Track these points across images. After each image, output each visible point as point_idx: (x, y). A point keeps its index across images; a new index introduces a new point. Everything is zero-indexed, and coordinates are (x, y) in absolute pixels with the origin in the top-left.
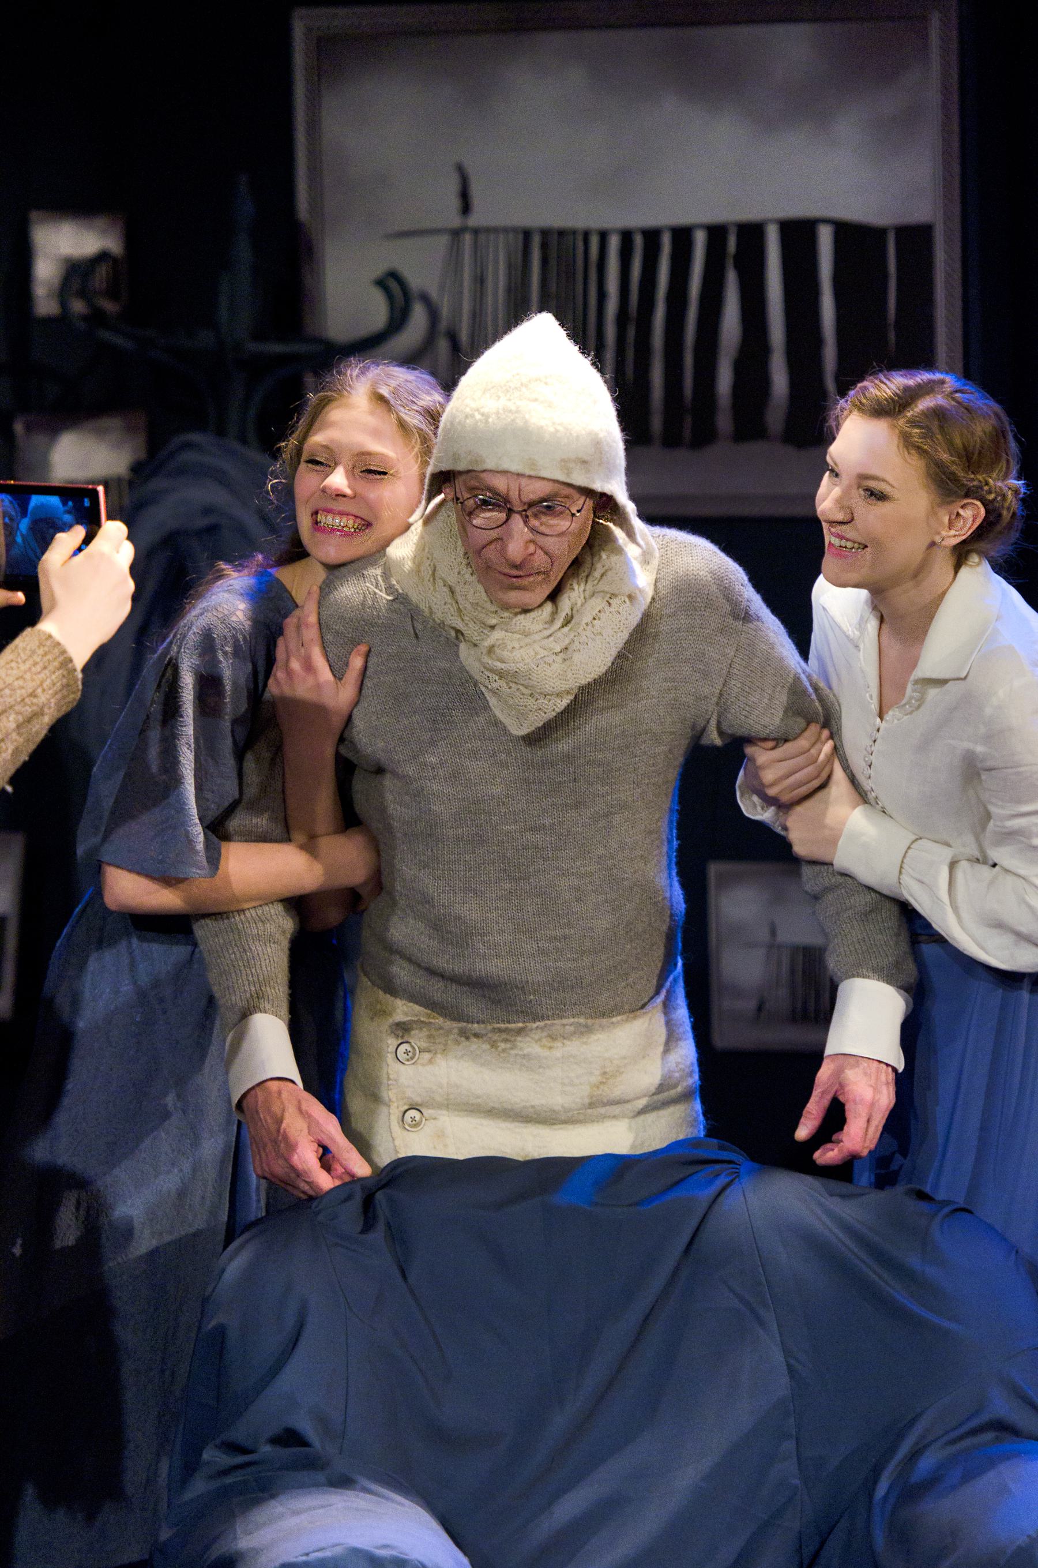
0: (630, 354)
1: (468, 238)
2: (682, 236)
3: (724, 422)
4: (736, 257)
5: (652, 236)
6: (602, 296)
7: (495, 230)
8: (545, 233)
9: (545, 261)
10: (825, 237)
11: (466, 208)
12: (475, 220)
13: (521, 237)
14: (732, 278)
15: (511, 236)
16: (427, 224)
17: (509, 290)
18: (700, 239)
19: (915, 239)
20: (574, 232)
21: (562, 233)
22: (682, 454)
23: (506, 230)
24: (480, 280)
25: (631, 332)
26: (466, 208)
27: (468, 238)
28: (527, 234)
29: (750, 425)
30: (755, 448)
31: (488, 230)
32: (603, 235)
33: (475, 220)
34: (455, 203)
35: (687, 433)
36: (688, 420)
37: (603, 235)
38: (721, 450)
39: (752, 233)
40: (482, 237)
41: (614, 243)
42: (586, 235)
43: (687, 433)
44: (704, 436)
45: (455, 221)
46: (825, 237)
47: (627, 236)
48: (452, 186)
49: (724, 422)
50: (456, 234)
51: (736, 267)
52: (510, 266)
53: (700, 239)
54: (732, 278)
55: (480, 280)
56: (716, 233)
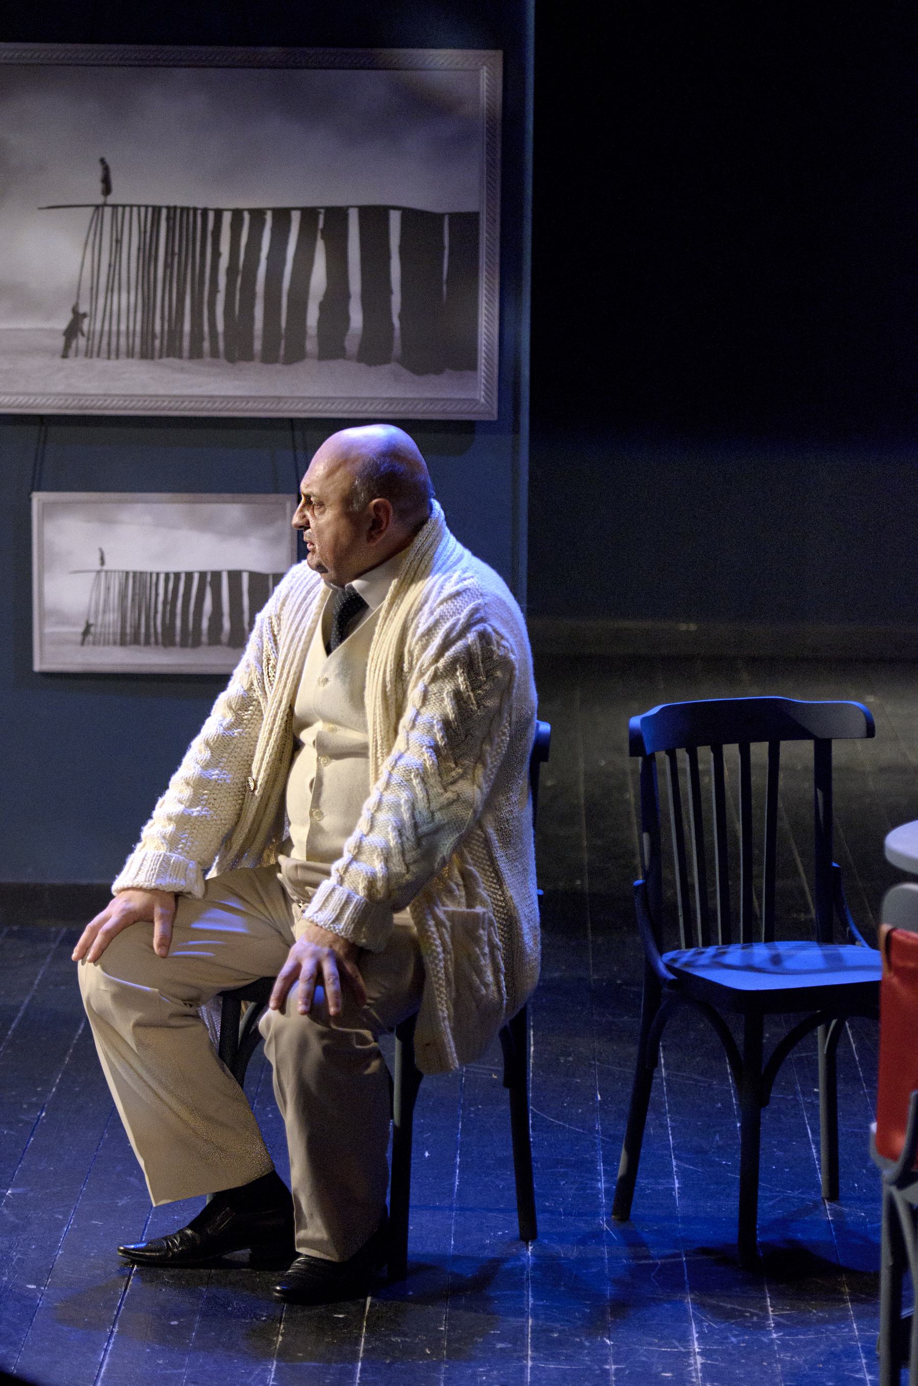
1: (108, 211)
7: (131, 206)
10: (395, 219)
11: (107, 190)
12: (111, 200)
13: (150, 210)
15: (143, 210)
19: (465, 223)
20: (195, 209)
22: (278, 366)
23: (139, 206)
24: (119, 242)
26: (107, 190)
27: (108, 211)
28: (157, 210)
29: (332, 347)
30: (337, 365)
31: (124, 206)
32: (219, 213)
33: (111, 200)
34: (99, 186)
35: (282, 352)
38: (310, 364)
42: (205, 212)
43: (282, 352)
45: (100, 200)
46: (395, 219)
48: (98, 173)
52: (142, 233)
54: (320, 246)
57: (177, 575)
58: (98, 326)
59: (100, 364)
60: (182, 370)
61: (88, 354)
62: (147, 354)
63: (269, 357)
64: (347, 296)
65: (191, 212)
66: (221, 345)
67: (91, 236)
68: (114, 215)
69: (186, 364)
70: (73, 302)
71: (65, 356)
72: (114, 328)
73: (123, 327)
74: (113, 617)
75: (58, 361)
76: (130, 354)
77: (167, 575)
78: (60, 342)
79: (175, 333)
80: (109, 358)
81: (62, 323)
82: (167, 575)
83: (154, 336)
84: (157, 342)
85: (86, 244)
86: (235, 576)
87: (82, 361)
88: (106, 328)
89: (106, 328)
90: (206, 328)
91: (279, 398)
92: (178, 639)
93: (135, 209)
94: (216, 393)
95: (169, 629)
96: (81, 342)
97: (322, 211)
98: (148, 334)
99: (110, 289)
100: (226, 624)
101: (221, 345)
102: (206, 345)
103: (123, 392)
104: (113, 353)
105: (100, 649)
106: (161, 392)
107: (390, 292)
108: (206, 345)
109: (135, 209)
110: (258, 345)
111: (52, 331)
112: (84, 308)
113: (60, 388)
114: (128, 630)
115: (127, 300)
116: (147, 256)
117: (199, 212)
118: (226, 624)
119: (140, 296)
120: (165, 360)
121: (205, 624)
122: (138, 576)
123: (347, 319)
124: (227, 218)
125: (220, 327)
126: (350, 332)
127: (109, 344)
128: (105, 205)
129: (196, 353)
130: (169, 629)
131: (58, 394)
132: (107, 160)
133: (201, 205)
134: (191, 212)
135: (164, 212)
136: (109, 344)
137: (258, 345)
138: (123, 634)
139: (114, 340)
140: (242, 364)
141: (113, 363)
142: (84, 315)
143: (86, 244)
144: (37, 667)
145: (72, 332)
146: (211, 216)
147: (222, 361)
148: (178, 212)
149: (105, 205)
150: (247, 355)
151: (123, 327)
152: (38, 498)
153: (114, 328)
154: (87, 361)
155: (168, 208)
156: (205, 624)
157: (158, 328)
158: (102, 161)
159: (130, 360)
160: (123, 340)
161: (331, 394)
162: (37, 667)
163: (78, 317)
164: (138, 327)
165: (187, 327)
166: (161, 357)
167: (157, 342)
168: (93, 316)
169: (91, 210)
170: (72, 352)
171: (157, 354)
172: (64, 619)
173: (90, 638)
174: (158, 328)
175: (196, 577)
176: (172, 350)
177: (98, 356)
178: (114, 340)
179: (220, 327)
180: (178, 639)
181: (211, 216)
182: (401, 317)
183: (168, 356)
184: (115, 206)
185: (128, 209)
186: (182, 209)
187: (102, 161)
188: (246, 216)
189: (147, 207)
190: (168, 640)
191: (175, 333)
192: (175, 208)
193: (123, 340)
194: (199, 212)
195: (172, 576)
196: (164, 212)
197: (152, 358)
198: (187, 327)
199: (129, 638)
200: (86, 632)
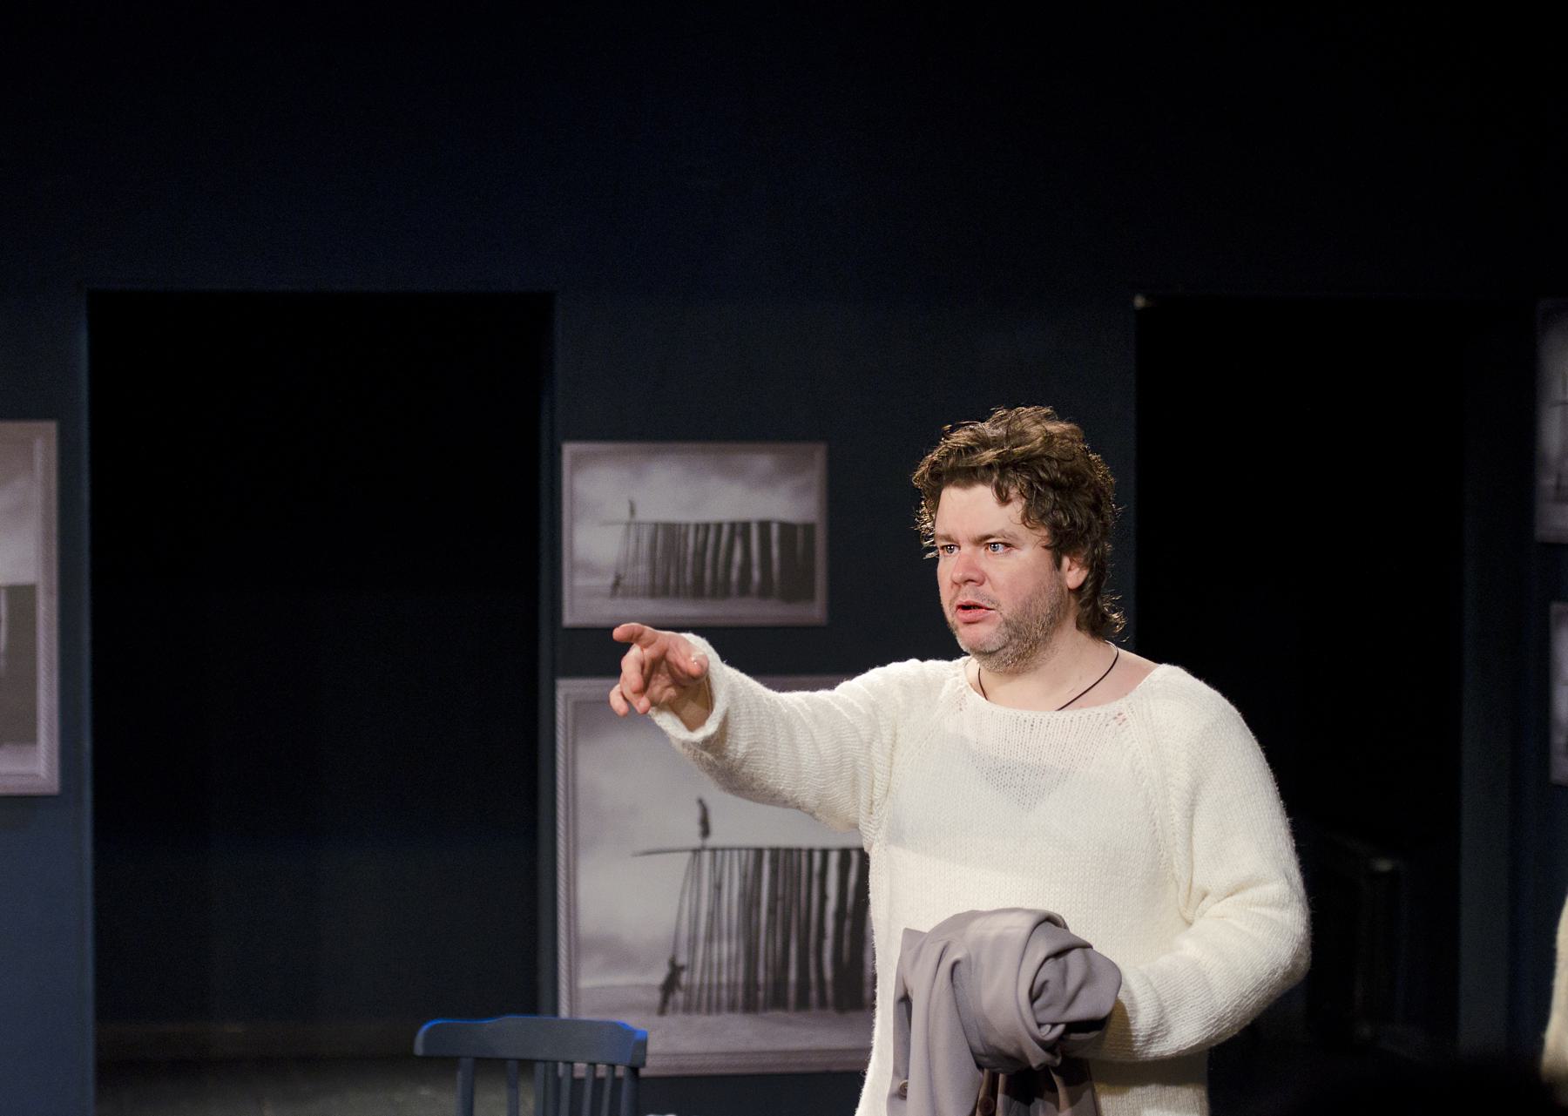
0: (846, 943)
1: (707, 855)
7: (731, 849)
8: (775, 851)
11: (706, 831)
13: (752, 854)
16: (677, 844)
17: (743, 895)
20: (800, 850)
21: (789, 851)
23: (740, 849)
24: (718, 887)
25: (848, 925)
26: (706, 831)
27: (707, 855)
28: (759, 852)
31: (723, 849)
32: (825, 853)
34: (696, 828)
37: (825, 853)
40: (719, 853)
41: (834, 858)
42: (810, 852)
45: (697, 842)
48: (696, 813)
50: (696, 852)
52: (744, 877)
55: (718, 887)
59: (700, 1020)
60: (789, 1023)
61: (687, 1009)
66: (830, 993)
68: (714, 859)
70: (668, 955)
71: (662, 1011)
72: (715, 980)
73: (724, 979)
76: (732, 1007)
78: (657, 997)
79: (779, 985)
80: (709, 1011)
81: (659, 976)
83: (757, 987)
87: (680, 1016)
96: (679, 996)
98: (751, 985)
99: (709, 939)
101: (830, 993)
102: (814, 994)
104: (714, 1007)
108: (814, 994)
111: (648, 987)
112: (682, 960)
120: (770, 1014)
129: (803, 1003)
135: (767, 855)
136: (709, 998)
140: (852, 1015)
141: (712, 1020)
142: (682, 968)
145: (670, 985)
146: (817, 857)
147: (831, 1011)
158: (701, 802)
159: (731, 1016)
160: (724, 994)
163: (675, 970)
164: (741, 979)
165: (793, 975)
166: (765, 1009)
167: (761, 994)
168: (690, 967)
169: (688, 855)
170: (670, 1007)
171: (761, 1004)
176: (778, 1000)
181: (817, 857)
184: (714, 850)
187: (701, 802)
189: (747, 849)
191: (779, 985)
196: (767, 855)
198: (793, 975)
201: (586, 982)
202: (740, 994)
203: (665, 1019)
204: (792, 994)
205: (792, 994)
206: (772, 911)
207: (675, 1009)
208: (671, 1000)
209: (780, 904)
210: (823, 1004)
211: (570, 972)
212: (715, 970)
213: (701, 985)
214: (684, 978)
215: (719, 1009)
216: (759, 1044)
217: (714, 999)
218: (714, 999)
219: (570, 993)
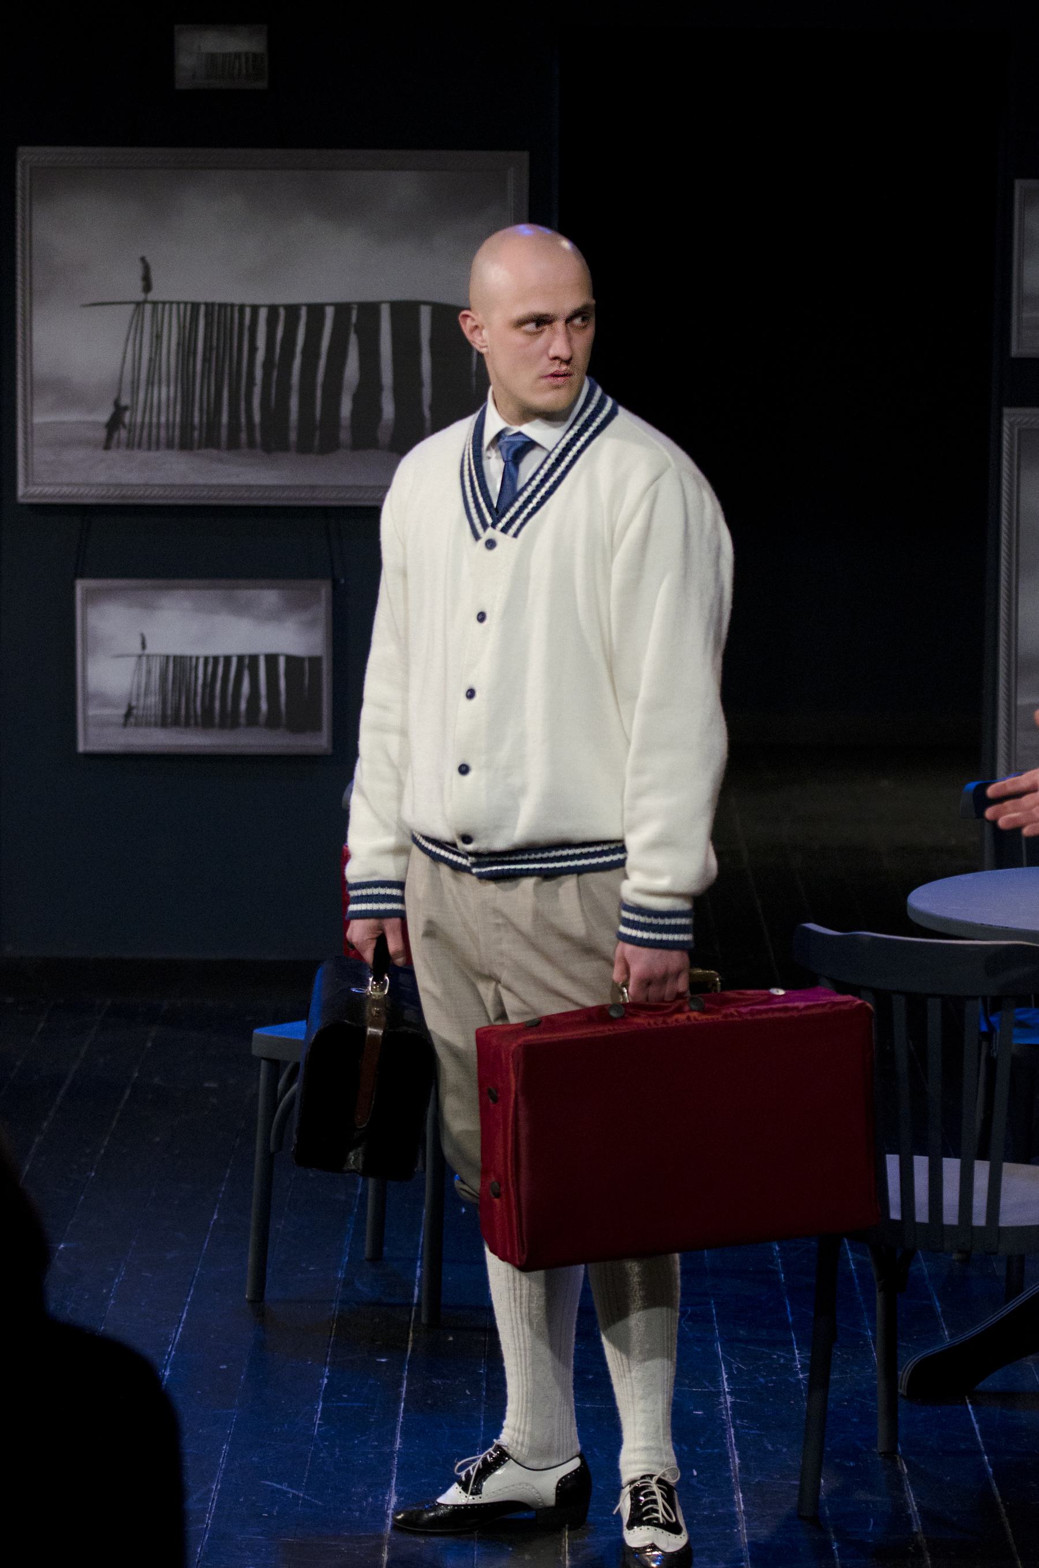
1: (148, 308)
2: (316, 311)
3: (345, 436)
4: (355, 326)
5: (292, 310)
6: (253, 349)
7: (171, 303)
9: (208, 325)
10: (425, 313)
11: (147, 287)
12: (152, 296)
13: (189, 307)
14: (353, 339)
15: (182, 306)
18: (330, 312)
20: (232, 306)
21: (222, 306)
23: (178, 303)
24: (159, 337)
26: (147, 287)
27: (148, 308)
28: (195, 306)
31: (164, 303)
32: (255, 309)
33: (152, 296)
34: (140, 284)
35: (316, 442)
36: (318, 433)
37: (255, 309)
39: (370, 310)
40: (160, 306)
41: (263, 313)
42: (242, 307)
43: (316, 442)
44: (329, 445)
45: (140, 297)
46: (425, 313)
47: (273, 310)
48: (138, 271)
49: (345, 436)
50: (138, 304)
51: (356, 332)
52: (181, 328)
53: (330, 312)
54: (353, 339)
56: (342, 309)
57: (216, 659)
58: (139, 419)
59: (141, 455)
60: (220, 460)
61: (130, 445)
62: (186, 445)
63: (304, 448)
64: (379, 388)
65: (229, 309)
67: (132, 332)
69: (224, 455)
70: (115, 396)
71: (107, 447)
72: (154, 420)
73: (163, 419)
74: (153, 700)
75: (101, 453)
76: (170, 445)
77: (206, 659)
78: (102, 434)
79: (212, 424)
80: (149, 449)
81: (104, 416)
82: (206, 659)
83: (193, 428)
84: (196, 434)
85: (127, 340)
86: (272, 659)
88: (147, 419)
89: (147, 419)
90: (243, 420)
91: (313, 487)
92: (217, 720)
93: (174, 306)
94: (253, 482)
95: (208, 710)
96: (123, 434)
97: (355, 306)
98: (187, 425)
99: (150, 383)
100: (264, 706)
102: (243, 436)
103: (164, 482)
104: (154, 444)
105: (142, 731)
106: (201, 481)
107: (420, 384)
108: (243, 436)
109: (174, 306)
110: (293, 436)
111: (94, 424)
112: (125, 401)
113: (102, 479)
114: (169, 712)
115: (166, 393)
116: (186, 350)
117: (236, 309)
118: (264, 706)
119: (179, 389)
120: (203, 451)
121: (243, 706)
122: (180, 661)
123: (379, 410)
124: (263, 313)
125: (257, 418)
126: (383, 423)
127: (150, 435)
128: (145, 302)
129: (233, 444)
130: (208, 710)
131: (100, 485)
132: (148, 259)
133: (237, 300)
134: (229, 309)
135: (202, 309)
136: (150, 435)
137: (293, 436)
138: (164, 716)
139: (154, 431)
141: (153, 454)
142: (126, 408)
143: (127, 340)
144: (81, 748)
145: (114, 424)
146: (248, 311)
148: (216, 308)
149: (145, 302)
150: (283, 446)
151: (163, 419)
152: (81, 586)
153: (154, 420)
154: (128, 452)
155: (206, 304)
156: (243, 706)
157: (196, 420)
158: (143, 259)
160: (163, 433)
161: (365, 483)
162: (81, 748)
164: (178, 419)
165: (225, 419)
166: (199, 448)
167: (196, 434)
168: (133, 407)
169: (132, 307)
172: (106, 701)
173: (132, 720)
174: (196, 420)
175: (234, 661)
176: (210, 441)
177: (140, 446)
178: (154, 431)
179: (257, 418)
180: (217, 720)
181: (248, 311)
182: (431, 408)
183: (207, 446)
184: (155, 303)
185: (167, 306)
186: (220, 305)
187: (143, 259)
188: (282, 312)
189: (186, 303)
190: (207, 721)
191: (212, 424)
192: (213, 304)
193: (163, 433)
194: (236, 309)
195: (211, 661)
196: (202, 309)
197: (191, 449)
198: (225, 419)
199: (169, 720)
200: (128, 714)
201: (38, 419)
202: (177, 433)
203: (112, 454)
204: (224, 433)
205: (224, 433)
206: (206, 360)
207: (118, 446)
208: (116, 436)
209: (214, 352)
210: (251, 444)
211: (25, 408)
212: (155, 410)
213: (143, 423)
214: (127, 417)
215: (158, 448)
216: (195, 478)
217: (154, 438)
218: (154, 438)
219: (26, 427)
